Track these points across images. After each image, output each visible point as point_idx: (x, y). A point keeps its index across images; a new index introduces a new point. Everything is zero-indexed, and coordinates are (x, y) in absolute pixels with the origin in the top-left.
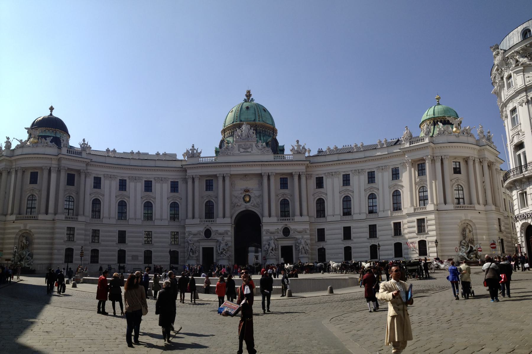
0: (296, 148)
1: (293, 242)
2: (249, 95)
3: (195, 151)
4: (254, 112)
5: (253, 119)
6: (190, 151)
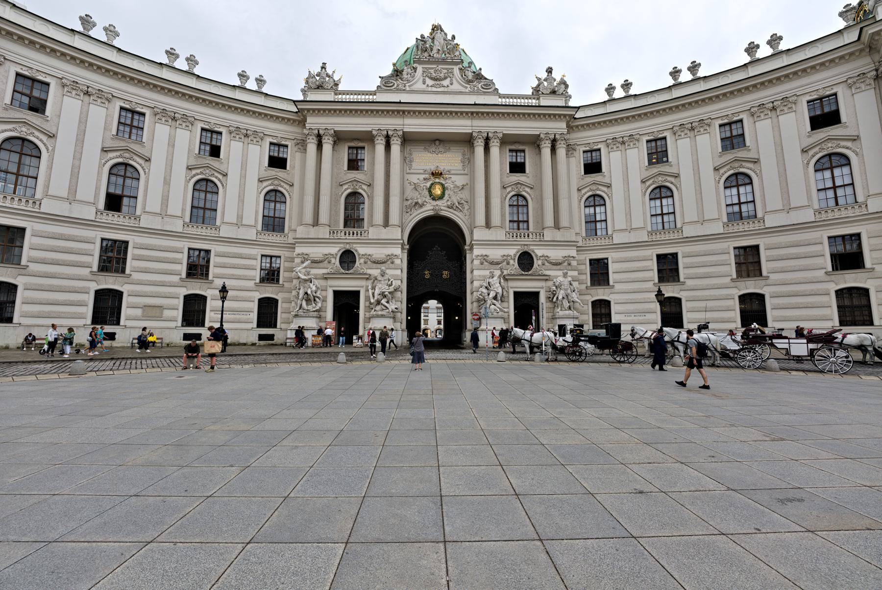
1: (542, 284)
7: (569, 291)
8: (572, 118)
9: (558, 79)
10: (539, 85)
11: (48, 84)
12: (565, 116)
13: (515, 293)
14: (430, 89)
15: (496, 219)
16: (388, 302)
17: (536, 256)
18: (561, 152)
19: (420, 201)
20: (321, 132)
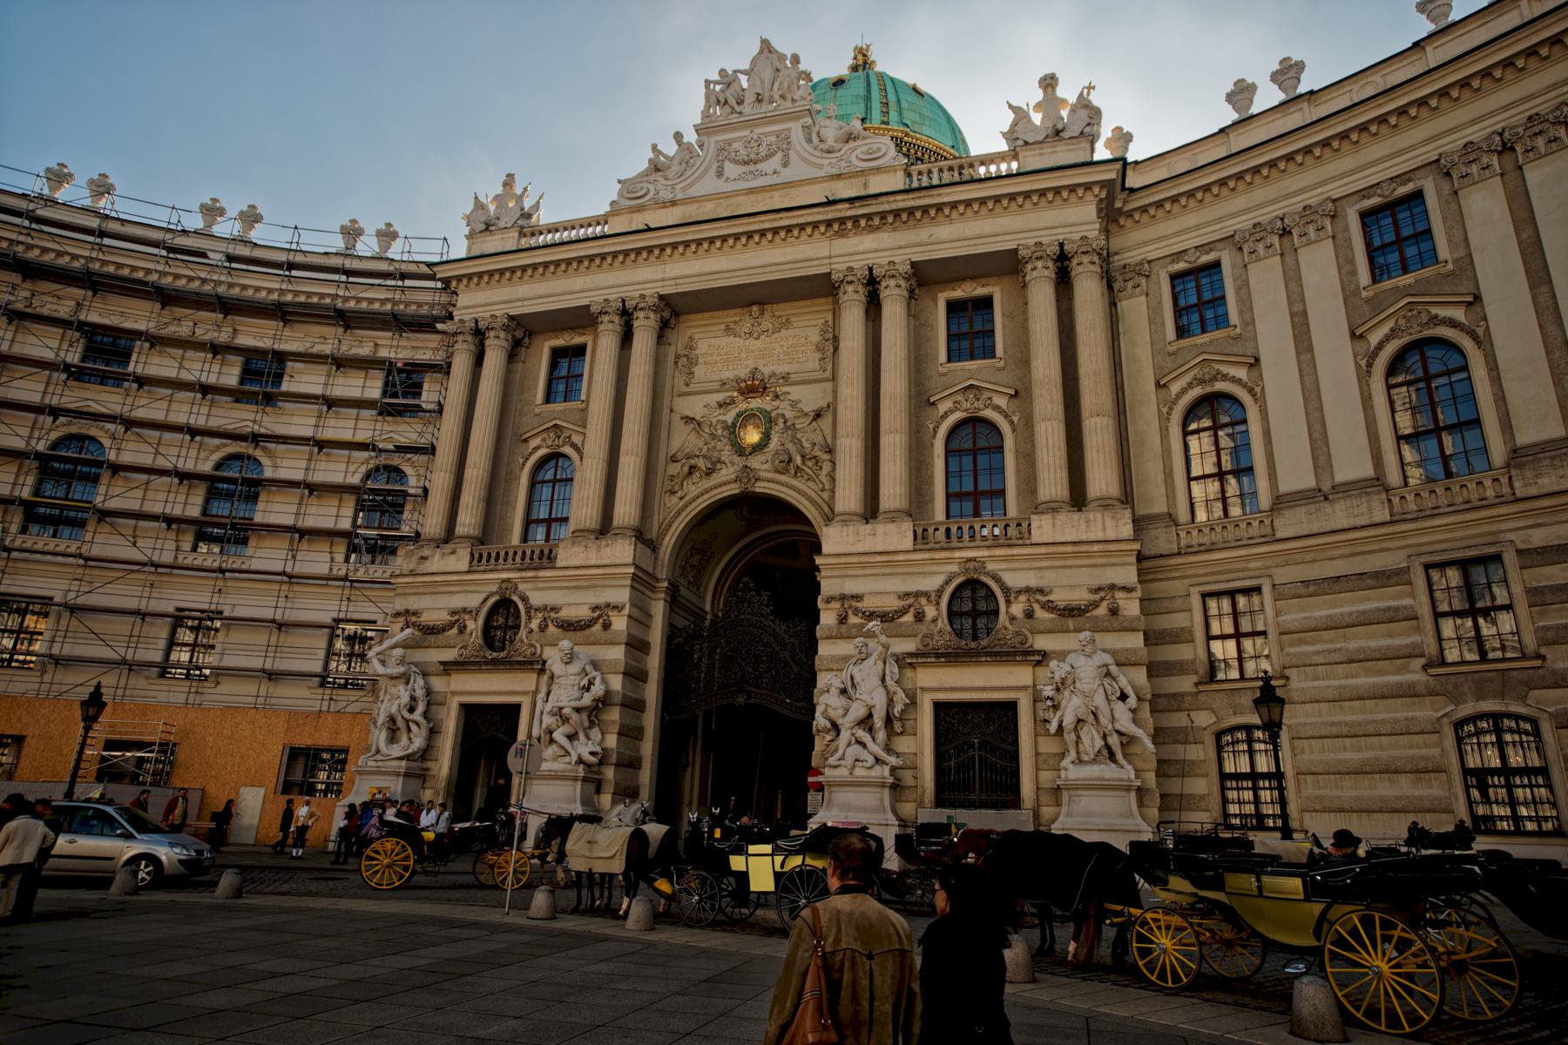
4: (862, 92)
7: (1099, 700)
8: (1119, 194)
9: (1072, 98)
10: (1015, 124)
12: (1088, 187)
13: (938, 706)
14: (731, 187)
15: (893, 492)
16: (572, 737)
17: (1007, 590)
18: (1088, 289)
19: (701, 463)
20: (482, 325)
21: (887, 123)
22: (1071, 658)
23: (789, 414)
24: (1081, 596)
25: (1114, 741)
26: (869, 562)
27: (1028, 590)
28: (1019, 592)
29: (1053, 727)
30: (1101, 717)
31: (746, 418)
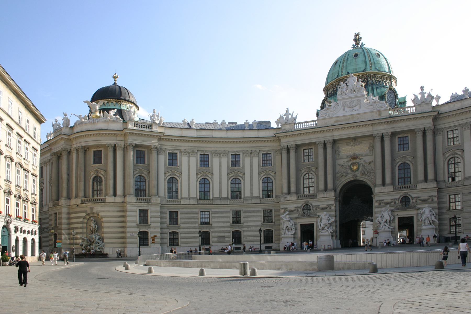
0: (419, 97)
1: (415, 212)
2: (357, 39)
3: (290, 116)
5: (362, 69)
6: (285, 117)
7: (429, 216)
11: (177, 153)
15: (388, 180)
17: (412, 197)
21: (372, 70)
22: (424, 209)
23: (363, 163)
24: (426, 198)
25: (431, 222)
26: (383, 194)
27: (416, 197)
28: (414, 198)
29: (421, 220)
30: (430, 218)
31: (353, 164)
